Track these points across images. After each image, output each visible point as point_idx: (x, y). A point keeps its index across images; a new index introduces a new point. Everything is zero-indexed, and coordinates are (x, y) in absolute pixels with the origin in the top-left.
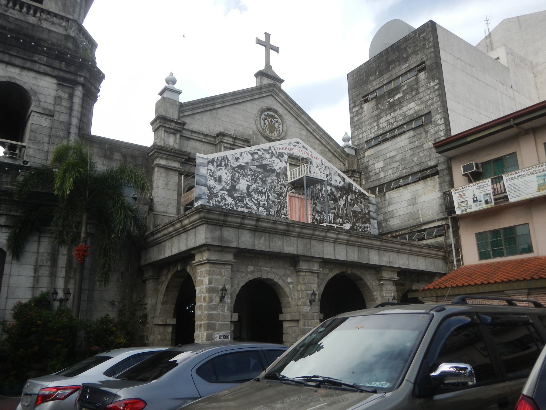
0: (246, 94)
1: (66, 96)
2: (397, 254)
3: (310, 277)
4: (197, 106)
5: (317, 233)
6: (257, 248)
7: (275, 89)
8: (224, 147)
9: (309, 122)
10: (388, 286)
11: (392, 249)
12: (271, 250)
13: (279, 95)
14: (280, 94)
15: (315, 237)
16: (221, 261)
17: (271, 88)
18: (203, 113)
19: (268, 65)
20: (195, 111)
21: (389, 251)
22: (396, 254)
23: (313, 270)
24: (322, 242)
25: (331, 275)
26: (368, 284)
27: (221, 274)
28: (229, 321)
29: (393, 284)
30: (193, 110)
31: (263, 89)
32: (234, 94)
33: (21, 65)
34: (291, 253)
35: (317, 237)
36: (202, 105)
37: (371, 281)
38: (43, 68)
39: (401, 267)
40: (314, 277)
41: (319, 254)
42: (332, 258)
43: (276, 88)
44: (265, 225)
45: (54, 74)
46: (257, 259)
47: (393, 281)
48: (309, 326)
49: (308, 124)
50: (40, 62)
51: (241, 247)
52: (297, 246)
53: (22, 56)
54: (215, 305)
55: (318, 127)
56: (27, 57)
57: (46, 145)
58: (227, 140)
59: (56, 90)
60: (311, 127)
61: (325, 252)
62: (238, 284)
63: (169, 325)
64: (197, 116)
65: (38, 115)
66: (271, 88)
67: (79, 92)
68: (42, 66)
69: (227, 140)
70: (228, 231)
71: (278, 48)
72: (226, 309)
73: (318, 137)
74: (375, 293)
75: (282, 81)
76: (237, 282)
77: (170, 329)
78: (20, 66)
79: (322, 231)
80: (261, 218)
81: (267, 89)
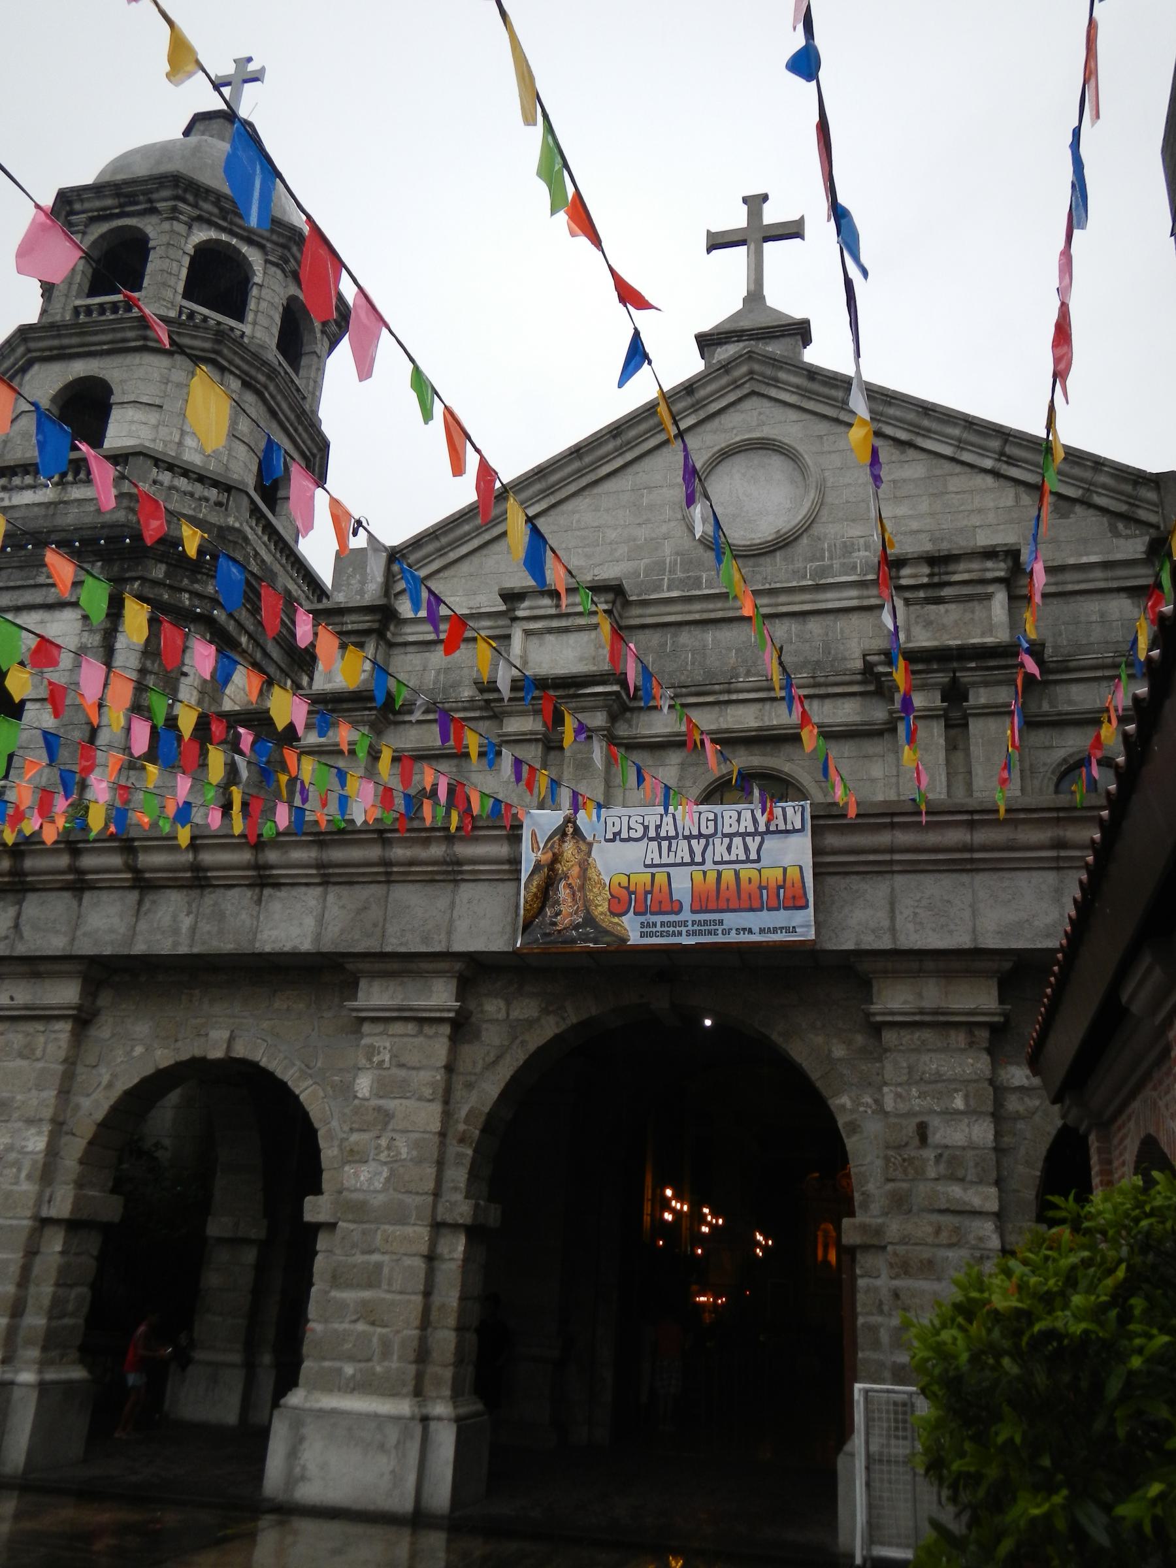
0: (632, 433)
2: (965, 878)
3: (406, 1039)
4: (452, 536)
5: (399, 852)
6: (139, 948)
7: (757, 367)
8: (528, 633)
9: (926, 423)
10: (925, 1058)
11: (897, 857)
12: (196, 950)
13: (777, 380)
14: (782, 375)
15: (402, 869)
17: (744, 369)
18: (484, 552)
19: (755, 296)
20: (453, 556)
21: (893, 872)
22: (947, 881)
23: (411, 1010)
24: (451, 886)
25: (549, 1029)
26: (799, 1052)
27: (33, 1051)
29: (971, 1044)
30: (446, 553)
31: (704, 386)
32: (576, 452)
33: (11, 604)
34: (287, 949)
35: (413, 869)
36: (467, 528)
37: (820, 1040)
39: (991, 942)
40: (430, 1037)
41: (426, 939)
42: (494, 947)
43: (759, 362)
44: (159, 859)
46: (197, 992)
47: (970, 1027)
48: (371, 1252)
49: (927, 433)
51: (80, 953)
52: (320, 921)
53: (12, 584)
55: (970, 423)
56: (19, 583)
58: (531, 608)
60: (944, 438)
61: (462, 926)
62: (110, 1085)
63: (246, 1241)
64: (465, 567)
65: (38, 705)
66: (744, 369)
69: (531, 608)
70: (43, 902)
71: (800, 222)
72: (23, 1174)
73: (988, 463)
74: (845, 1100)
75: (801, 331)
76: (106, 1079)
77: (250, 1256)
78: (9, 607)
79: (426, 842)
80: (133, 840)
81: (724, 380)
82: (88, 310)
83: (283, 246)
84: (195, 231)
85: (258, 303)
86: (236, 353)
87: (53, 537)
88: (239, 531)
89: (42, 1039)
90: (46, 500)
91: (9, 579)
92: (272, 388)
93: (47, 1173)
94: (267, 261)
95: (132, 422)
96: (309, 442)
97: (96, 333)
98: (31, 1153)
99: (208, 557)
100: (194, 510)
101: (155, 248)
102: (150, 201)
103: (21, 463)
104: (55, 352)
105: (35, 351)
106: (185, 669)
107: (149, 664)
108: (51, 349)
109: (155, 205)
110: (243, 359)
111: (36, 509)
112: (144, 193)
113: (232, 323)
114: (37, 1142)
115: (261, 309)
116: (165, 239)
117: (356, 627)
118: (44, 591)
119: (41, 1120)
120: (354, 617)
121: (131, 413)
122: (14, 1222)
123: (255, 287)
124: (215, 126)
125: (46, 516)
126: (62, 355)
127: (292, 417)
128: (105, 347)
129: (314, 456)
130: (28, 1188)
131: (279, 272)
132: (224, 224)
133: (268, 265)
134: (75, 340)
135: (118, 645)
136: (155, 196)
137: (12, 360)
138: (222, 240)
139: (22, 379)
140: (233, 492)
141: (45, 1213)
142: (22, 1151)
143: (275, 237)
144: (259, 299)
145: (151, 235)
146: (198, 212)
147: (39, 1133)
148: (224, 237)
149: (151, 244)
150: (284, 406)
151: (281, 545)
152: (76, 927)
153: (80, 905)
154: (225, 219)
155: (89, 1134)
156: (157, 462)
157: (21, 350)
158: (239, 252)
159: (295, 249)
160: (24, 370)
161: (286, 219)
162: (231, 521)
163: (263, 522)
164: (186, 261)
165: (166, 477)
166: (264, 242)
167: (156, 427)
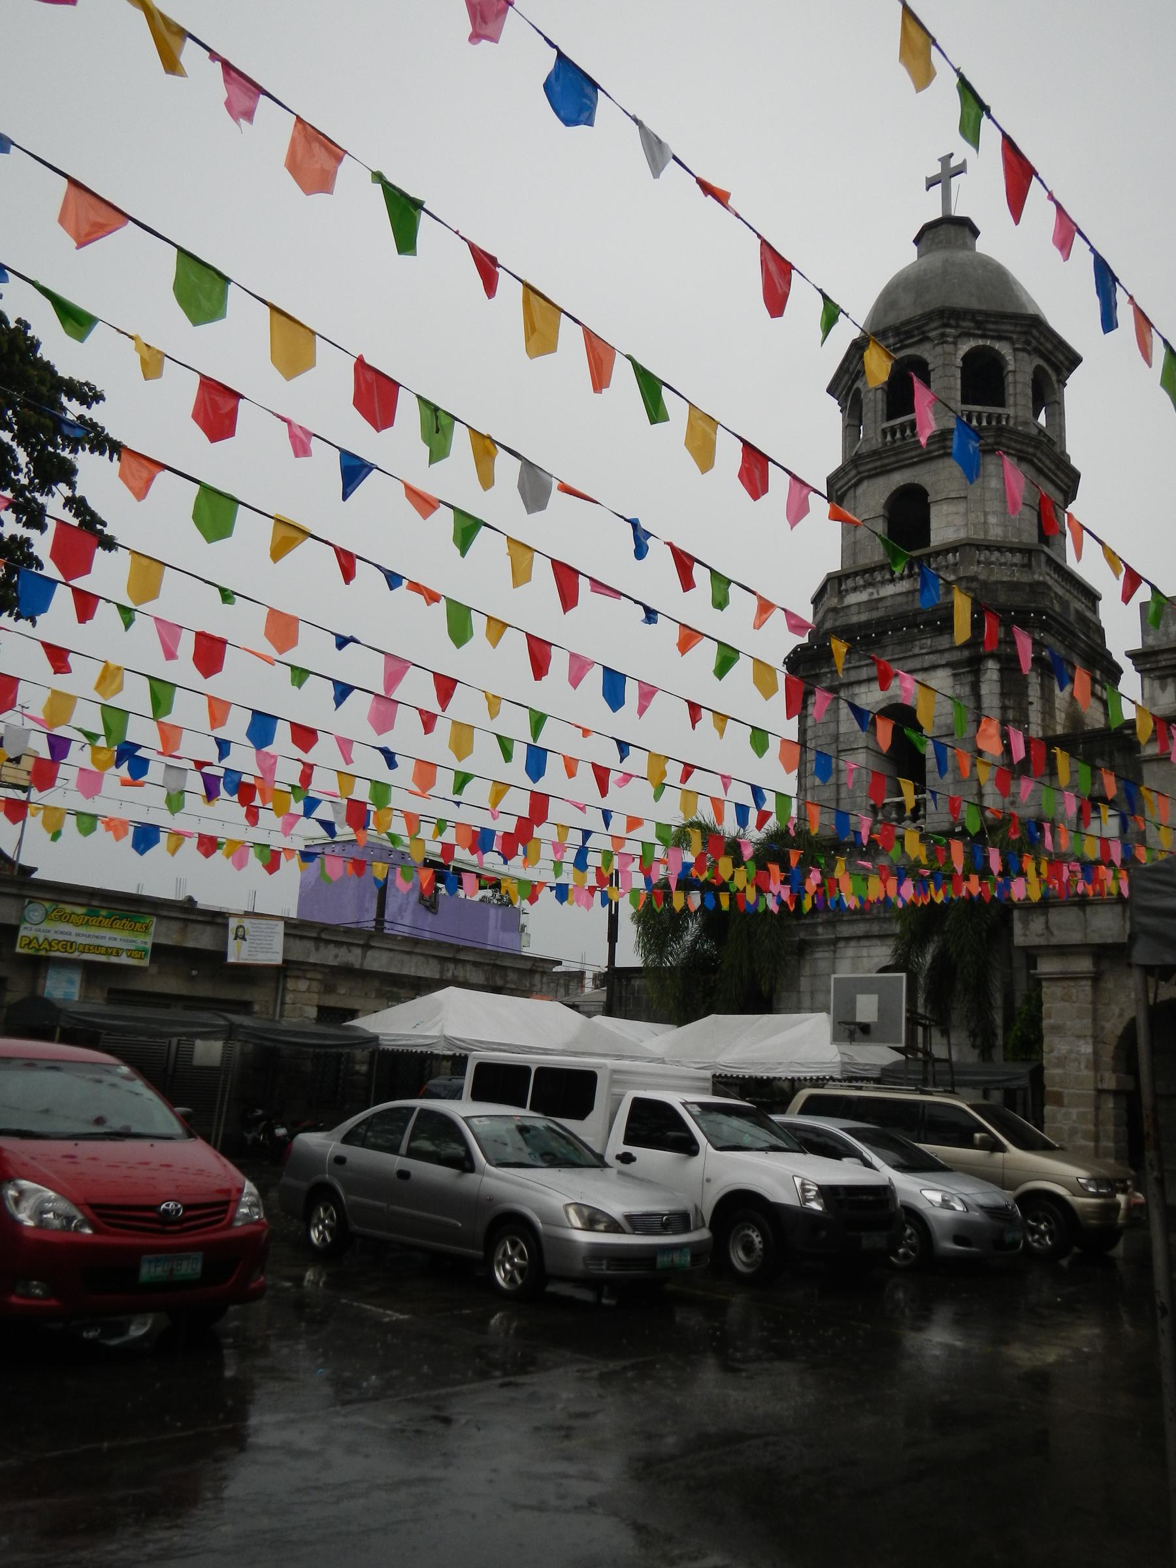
1: (966, 690)
16: (1061, 973)
28: (1090, 1090)
38: (929, 660)
45: (943, 662)
50: (924, 651)
51: (1092, 942)
53: (896, 656)
54: (1058, 1058)
56: (901, 656)
57: (951, 787)
59: (953, 687)
62: (1121, 1015)
67: (991, 671)
68: (927, 657)
72: (1083, 1066)
76: (1117, 1011)
82: (893, 431)
83: (1025, 333)
84: (960, 346)
85: (1015, 387)
86: (1011, 439)
87: (919, 619)
88: (1044, 583)
89: (1074, 991)
90: (904, 591)
91: (893, 654)
92: (1039, 454)
93: (1096, 1064)
94: (1015, 350)
95: (948, 515)
96: (1066, 480)
97: (907, 451)
98: (1085, 1054)
99: (1032, 615)
100: (1010, 576)
101: (934, 370)
102: (923, 333)
103: (879, 564)
104: (879, 470)
105: (864, 472)
106: (1030, 700)
107: (1007, 702)
108: (875, 468)
109: (927, 334)
110: (1016, 441)
111: (899, 598)
112: (918, 328)
113: (999, 410)
114: (1087, 1048)
115: (1018, 391)
116: (940, 361)
117: (1168, 663)
118: (920, 658)
119: (1085, 1036)
120: (1166, 656)
121: (946, 508)
122: (1084, 1092)
123: (1010, 374)
124: (941, 232)
125: (907, 603)
126: (884, 471)
127: (1053, 467)
128: (915, 460)
129: (1069, 487)
130: (1087, 1073)
131: (1025, 355)
132: (980, 332)
133: (1017, 352)
134: (892, 459)
135: (983, 692)
136: (926, 329)
137: (846, 479)
138: (980, 346)
139: (855, 492)
140: (1033, 553)
141: (1100, 1086)
142: (1078, 1053)
143: (1018, 329)
144: (1015, 383)
145: (929, 360)
146: (960, 331)
147: (1086, 1043)
148: (981, 342)
149: (931, 367)
150: (1048, 462)
151: (1066, 576)
152: (1086, 928)
153: (1085, 915)
154: (979, 328)
155: (1115, 1044)
156: (979, 546)
157: (853, 472)
158: (991, 349)
159: (1035, 332)
160: (856, 485)
161: (1024, 311)
162: (1036, 577)
163: (1054, 565)
164: (958, 373)
165: (983, 556)
166: (1011, 335)
167: (966, 514)
